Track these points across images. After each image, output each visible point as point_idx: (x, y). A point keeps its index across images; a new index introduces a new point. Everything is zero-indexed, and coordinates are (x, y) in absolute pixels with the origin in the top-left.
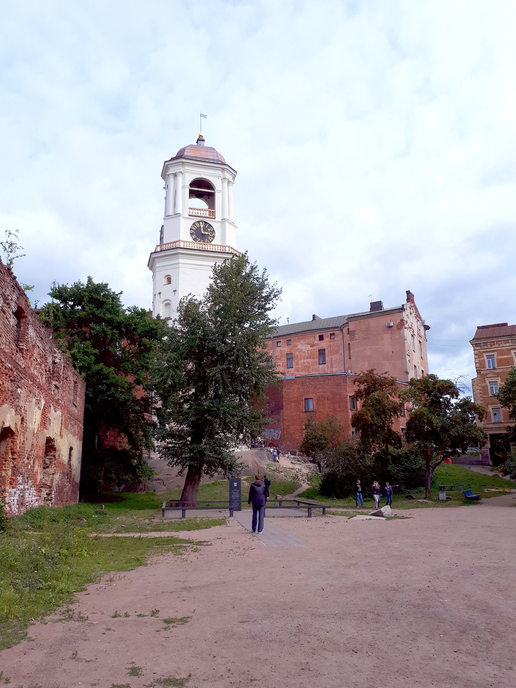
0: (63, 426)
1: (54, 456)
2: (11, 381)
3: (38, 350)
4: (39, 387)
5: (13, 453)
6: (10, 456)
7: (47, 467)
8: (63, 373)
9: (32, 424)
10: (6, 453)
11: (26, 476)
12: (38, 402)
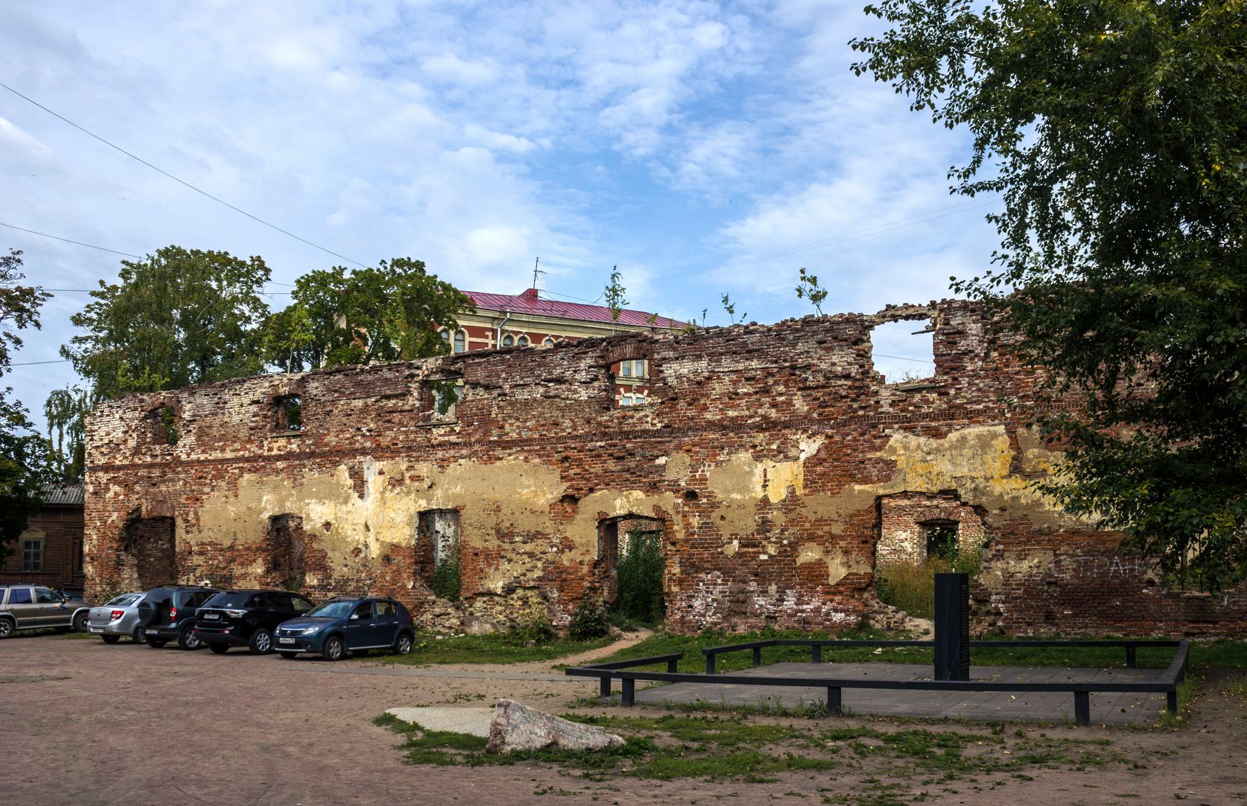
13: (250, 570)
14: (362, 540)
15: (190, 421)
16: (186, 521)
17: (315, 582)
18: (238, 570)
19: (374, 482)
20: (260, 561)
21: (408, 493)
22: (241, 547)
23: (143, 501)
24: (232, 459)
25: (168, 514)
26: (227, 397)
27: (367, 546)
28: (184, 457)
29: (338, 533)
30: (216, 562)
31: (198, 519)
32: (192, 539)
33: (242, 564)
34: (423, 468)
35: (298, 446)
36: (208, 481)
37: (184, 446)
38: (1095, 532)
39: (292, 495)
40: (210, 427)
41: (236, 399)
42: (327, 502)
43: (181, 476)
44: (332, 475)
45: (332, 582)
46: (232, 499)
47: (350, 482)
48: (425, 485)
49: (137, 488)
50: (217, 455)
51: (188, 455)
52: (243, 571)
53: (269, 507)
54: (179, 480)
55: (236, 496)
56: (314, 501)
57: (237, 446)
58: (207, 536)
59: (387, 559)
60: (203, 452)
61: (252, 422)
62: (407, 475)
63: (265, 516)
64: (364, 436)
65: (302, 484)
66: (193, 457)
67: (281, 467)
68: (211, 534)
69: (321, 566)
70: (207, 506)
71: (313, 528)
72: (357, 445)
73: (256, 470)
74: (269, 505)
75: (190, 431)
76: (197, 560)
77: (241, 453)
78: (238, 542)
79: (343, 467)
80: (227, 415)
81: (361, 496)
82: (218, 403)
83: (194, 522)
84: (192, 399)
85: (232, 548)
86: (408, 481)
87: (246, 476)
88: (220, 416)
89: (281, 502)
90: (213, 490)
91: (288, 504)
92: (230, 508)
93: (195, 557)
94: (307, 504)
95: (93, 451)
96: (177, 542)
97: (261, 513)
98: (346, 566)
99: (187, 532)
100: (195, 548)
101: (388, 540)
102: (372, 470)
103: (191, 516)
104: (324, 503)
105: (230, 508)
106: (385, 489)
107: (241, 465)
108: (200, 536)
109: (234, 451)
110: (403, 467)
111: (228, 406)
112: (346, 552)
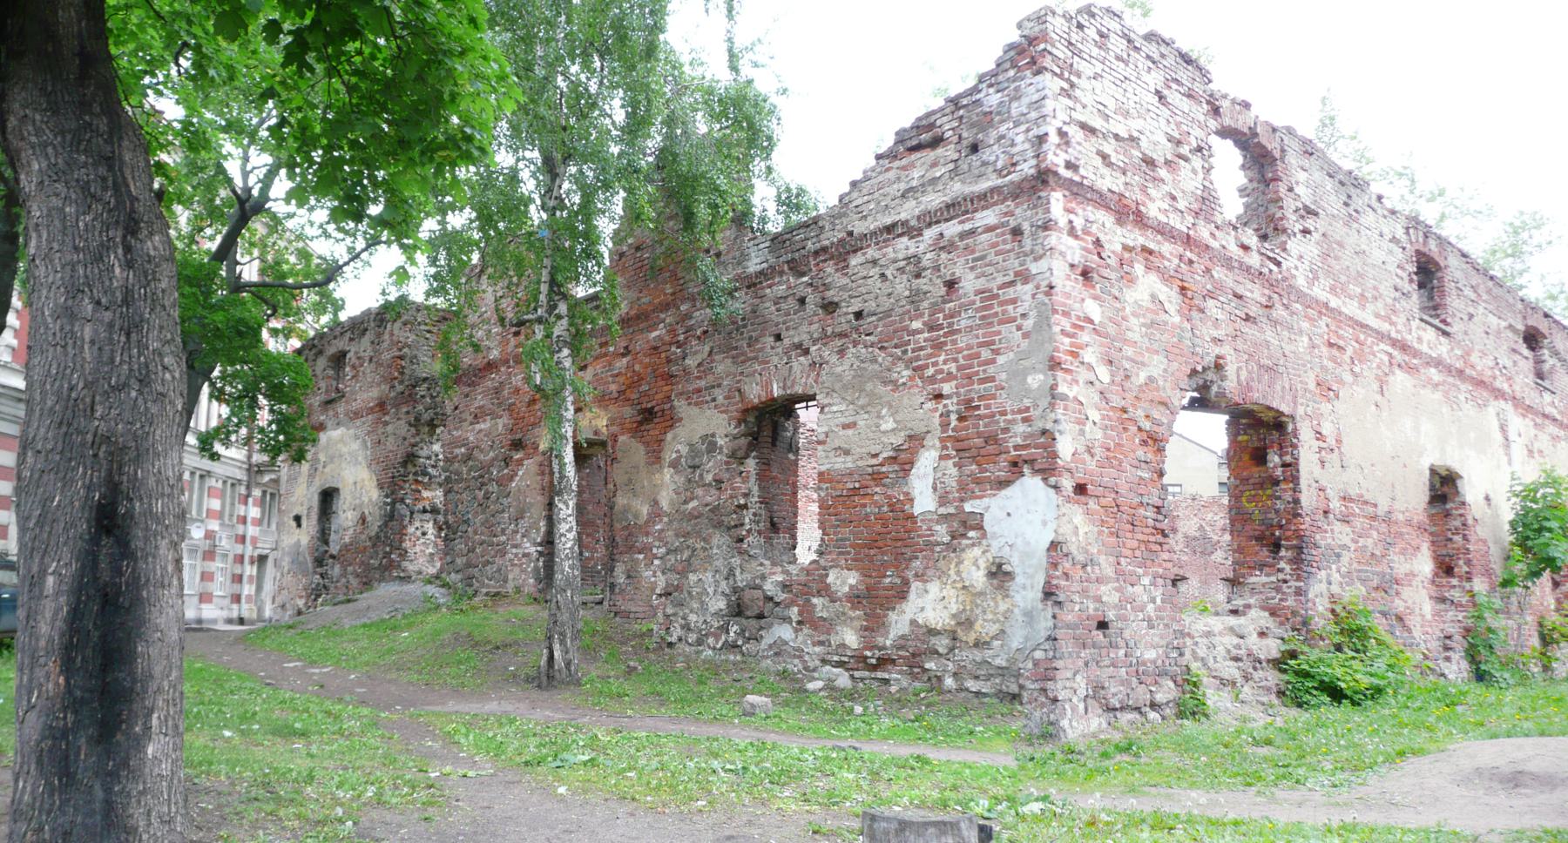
15: (1306, 207)
16: (1319, 436)
22: (1401, 517)
24: (1377, 332)
25: (1285, 409)
28: (1301, 282)
36: (1346, 358)
63: (1425, 463)
83: (1331, 441)
93: (1338, 526)
100: (1335, 505)
103: (1327, 429)
109: (1377, 316)
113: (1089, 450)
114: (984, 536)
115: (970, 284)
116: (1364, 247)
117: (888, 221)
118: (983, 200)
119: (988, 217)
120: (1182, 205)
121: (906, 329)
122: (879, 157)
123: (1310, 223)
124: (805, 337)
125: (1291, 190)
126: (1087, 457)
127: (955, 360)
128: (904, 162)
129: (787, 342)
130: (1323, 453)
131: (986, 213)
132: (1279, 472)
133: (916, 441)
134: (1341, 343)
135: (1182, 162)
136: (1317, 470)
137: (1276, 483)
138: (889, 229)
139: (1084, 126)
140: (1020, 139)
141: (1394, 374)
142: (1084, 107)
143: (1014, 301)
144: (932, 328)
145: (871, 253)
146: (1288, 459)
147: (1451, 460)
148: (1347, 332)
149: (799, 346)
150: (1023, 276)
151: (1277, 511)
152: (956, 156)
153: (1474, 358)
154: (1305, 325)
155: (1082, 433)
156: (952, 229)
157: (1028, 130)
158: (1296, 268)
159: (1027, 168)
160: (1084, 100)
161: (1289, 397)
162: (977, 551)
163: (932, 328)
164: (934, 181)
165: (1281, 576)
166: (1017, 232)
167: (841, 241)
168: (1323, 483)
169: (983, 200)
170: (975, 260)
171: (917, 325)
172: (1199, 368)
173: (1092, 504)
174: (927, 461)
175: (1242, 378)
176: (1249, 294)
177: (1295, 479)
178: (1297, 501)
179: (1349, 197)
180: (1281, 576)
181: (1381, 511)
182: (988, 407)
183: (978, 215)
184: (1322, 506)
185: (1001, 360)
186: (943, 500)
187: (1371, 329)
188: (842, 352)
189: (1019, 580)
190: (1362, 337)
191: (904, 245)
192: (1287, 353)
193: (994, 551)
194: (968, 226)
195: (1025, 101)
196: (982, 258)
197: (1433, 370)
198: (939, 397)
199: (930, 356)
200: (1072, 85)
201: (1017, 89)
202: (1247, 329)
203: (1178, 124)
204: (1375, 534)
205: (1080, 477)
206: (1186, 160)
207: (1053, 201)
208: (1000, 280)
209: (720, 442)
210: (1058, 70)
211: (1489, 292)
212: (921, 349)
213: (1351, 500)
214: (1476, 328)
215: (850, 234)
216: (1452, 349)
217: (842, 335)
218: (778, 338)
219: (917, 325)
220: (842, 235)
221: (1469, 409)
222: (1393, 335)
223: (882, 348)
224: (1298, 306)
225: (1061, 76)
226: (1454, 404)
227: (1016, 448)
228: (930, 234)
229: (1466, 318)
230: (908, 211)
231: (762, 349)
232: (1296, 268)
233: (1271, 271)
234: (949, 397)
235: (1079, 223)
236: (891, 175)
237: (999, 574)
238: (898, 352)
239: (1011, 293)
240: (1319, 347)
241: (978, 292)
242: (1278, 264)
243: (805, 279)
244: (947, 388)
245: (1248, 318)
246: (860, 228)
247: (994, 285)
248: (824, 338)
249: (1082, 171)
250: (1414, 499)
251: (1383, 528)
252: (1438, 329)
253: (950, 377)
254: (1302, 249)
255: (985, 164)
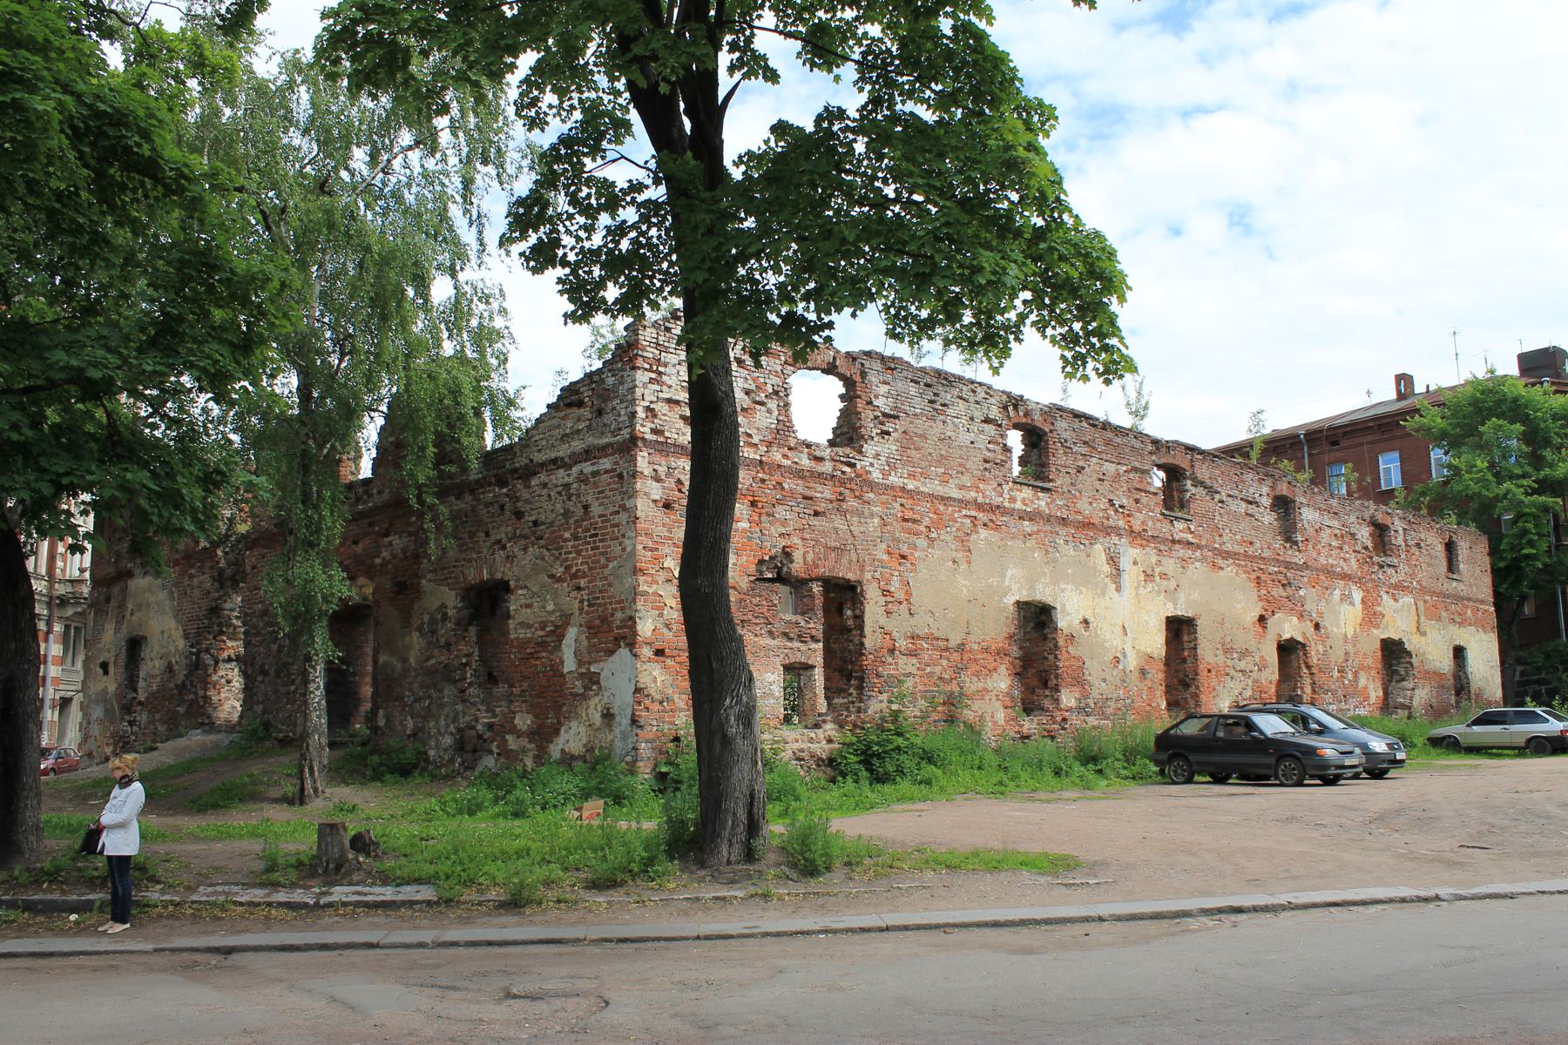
0: (1422, 619)
1: (1410, 663)
2: (1283, 585)
3: (1328, 531)
4: (1345, 577)
5: (1308, 667)
6: (1305, 671)
7: (1403, 680)
8: (1405, 541)
9: (1338, 626)
10: (1300, 668)
11: (1340, 693)
12: (1347, 598)
13: (990, 684)
14: (1119, 648)
15: (885, 415)
16: (886, 592)
17: (1073, 703)
18: (972, 684)
19: (1131, 575)
20: (1003, 669)
21: (1159, 592)
22: (976, 647)
23: (796, 540)
24: (961, 501)
25: (851, 576)
26: (949, 396)
27: (1124, 655)
28: (876, 475)
29: (1097, 635)
30: (938, 670)
31: (908, 594)
32: (900, 626)
33: (977, 674)
34: (1170, 566)
35: (1047, 504)
36: (922, 528)
37: (877, 456)
38: (230, 442)
39: (1044, 574)
40: (924, 437)
41: (962, 405)
42: (1083, 589)
43: (877, 509)
44: (1088, 556)
45: (1091, 702)
46: (963, 567)
47: (1107, 569)
48: (1173, 584)
49: (781, 512)
50: (934, 487)
51: (885, 475)
52: (980, 685)
53: (1015, 587)
54: (872, 515)
55: (969, 563)
56: (1069, 587)
57: (966, 480)
58: (921, 624)
59: (1143, 672)
60: (912, 476)
61: (989, 450)
62: (1157, 570)
63: (1011, 600)
64: (1117, 511)
65: (1055, 561)
66: (894, 479)
67: (1029, 530)
68: (931, 621)
69: (1080, 682)
70: (923, 573)
71: (1070, 626)
72: (1111, 523)
73: (997, 528)
74: (1016, 588)
75: (888, 433)
76: (906, 665)
77: (973, 494)
78: (972, 638)
79: (1098, 547)
80: (950, 427)
81: (1118, 589)
82: (931, 402)
83: (900, 595)
84: (889, 378)
85: (961, 648)
86: (1157, 578)
87: (984, 533)
88: (940, 425)
89: (1031, 583)
90: (931, 546)
91: (1040, 587)
92: (961, 580)
93: (902, 660)
94: (1063, 591)
95: (661, 408)
96: (868, 630)
97: (1005, 595)
98: (1104, 680)
99: (888, 613)
100: (902, 644)
101: (1143, 649)
102: (1130, 554)
104: (1081, 593)
105: (961, 580)
106: (1139, 585)
107: (973, 513)
108: (913, 621)
109: (961, 487)
110: (1154, 559)
111: (950, 411)
112: (1104, 662)
113: (667, 626)
114: (600, 689)
115: (596, 510)
116: (949, 434)
117: (553, 456)
118: (603, 450)
119: (606, 464)
120: (755, 440)
121: (561, 537)
122: (549, 406)
123: (889, 427)
124: (503, 535)
125: (870, 403)
126: (665, 630)
127: (587, 563)
128: (562, 414)
129: (493, 538)
130: (890, 606)
131: (605, 460)
132: (850, 623)
133: (566, 620)
134: (917, 517)
135: (758, 407)
136: (883, 620)
137: (850, 630)
138: (554, 461)
139: (669, 401)
140: (623, 412)
141: (977, 532)
142: (670, 387)
143: (616, 525)
144: (575, 537)
145: (543, 477)
146: (858, 612)
147: (1042, 593)
148: (923, 507)
149: (499, 542)
150: (623, 507)
151: (850, 651)
152: (590, 416)
153: (1082, 505)
154: (877, 509)
155: (661, 615)
156: (588, 468)
157: (627, 407)
158: (872, 465)
159: (625, 433)
160: (669, 383)
161: (855, 567)
162: (597, 699)
163: (575, 537)
164: (578, 432)
165: (851, 699)
166: (620, 476)
167: (526, 465)
168: (889, 628)
169: (603, 450)
170: (599, 493)
171: (567, 535)
172: (767, 558)
173: (669, 662)
174: (572, 633)
175: (809, 559)
176: (818, 495)
177: (861, 627)
178: (862, 644)
179: (936, 395)
180: (851, 699)
181: (952, 644)
182: (603, 598)
183: (601, 461)
184: (888, 644)
185: (611, 565)
186: (580, 663)
187: (954, 500)
188: (525, 549)
189: (617, 719)
190: (942, 508)
191: (561, 476)
192: (855, 533)
193: (605, 700)
194: (596, 468)
195: (626, 386)
196: (602, 492)
197: (1026, 523)
198: (579, 588)
199: (574, 559)
200: (660, 374)
201: (622, 377)
202: (815, 522)
203: (754, 380)
204: (945, 662)
205: (659, 645)
206: (762, 404)
207: (639, 459)
208: (612, 509)
209: (451, 612)
210: (647, 366)
211: (1108, 443)
212: (570, 553)
213: (919, 637)
214: (1088, 480)
215: (532, 460)
216: (1053, 501)
217: (525, 537)
218: (487, 534)
219: (567, 535)
220: (527, 461)
221: (1069, 550)
222: (980, 500)
223: (548, 550)
224: (871, 495)
225: (651, 370)
226: (1048, 549)
227: (618, 628)
228: (576, 469)
229: (1073, 472)
230: (563, 451)
231: (477, 542)
232: (872, 465)
233: (843, 473)
234: (583, 589)
235: (662, 470)
236: (554, 422)
237: (608, 716)
238: (557, 553)
239: (616, 518)
240: (891, 524)
241: (600, 516)
242: (852, 465)
243: (505, 490)
244: (583, 583)
245: (816, 514)
246: (539, 457)
247: (608, 512)
248: (514, 538)
249: (667, 434)
250: (997, 626)
251: (956, 656)
252: (1033, 486)
253: (584, 575)
254: (879, 449)
255: (605, 425)
